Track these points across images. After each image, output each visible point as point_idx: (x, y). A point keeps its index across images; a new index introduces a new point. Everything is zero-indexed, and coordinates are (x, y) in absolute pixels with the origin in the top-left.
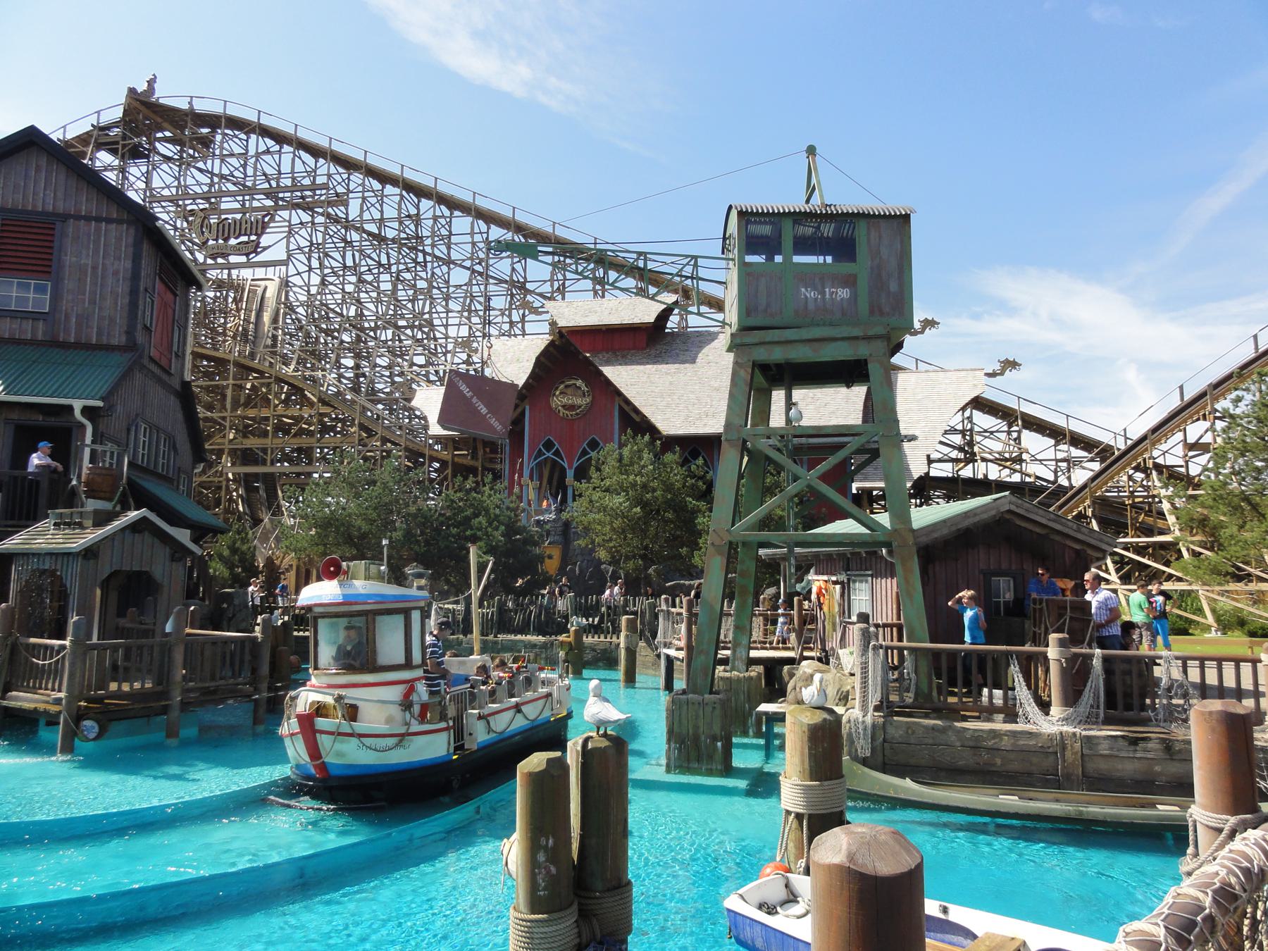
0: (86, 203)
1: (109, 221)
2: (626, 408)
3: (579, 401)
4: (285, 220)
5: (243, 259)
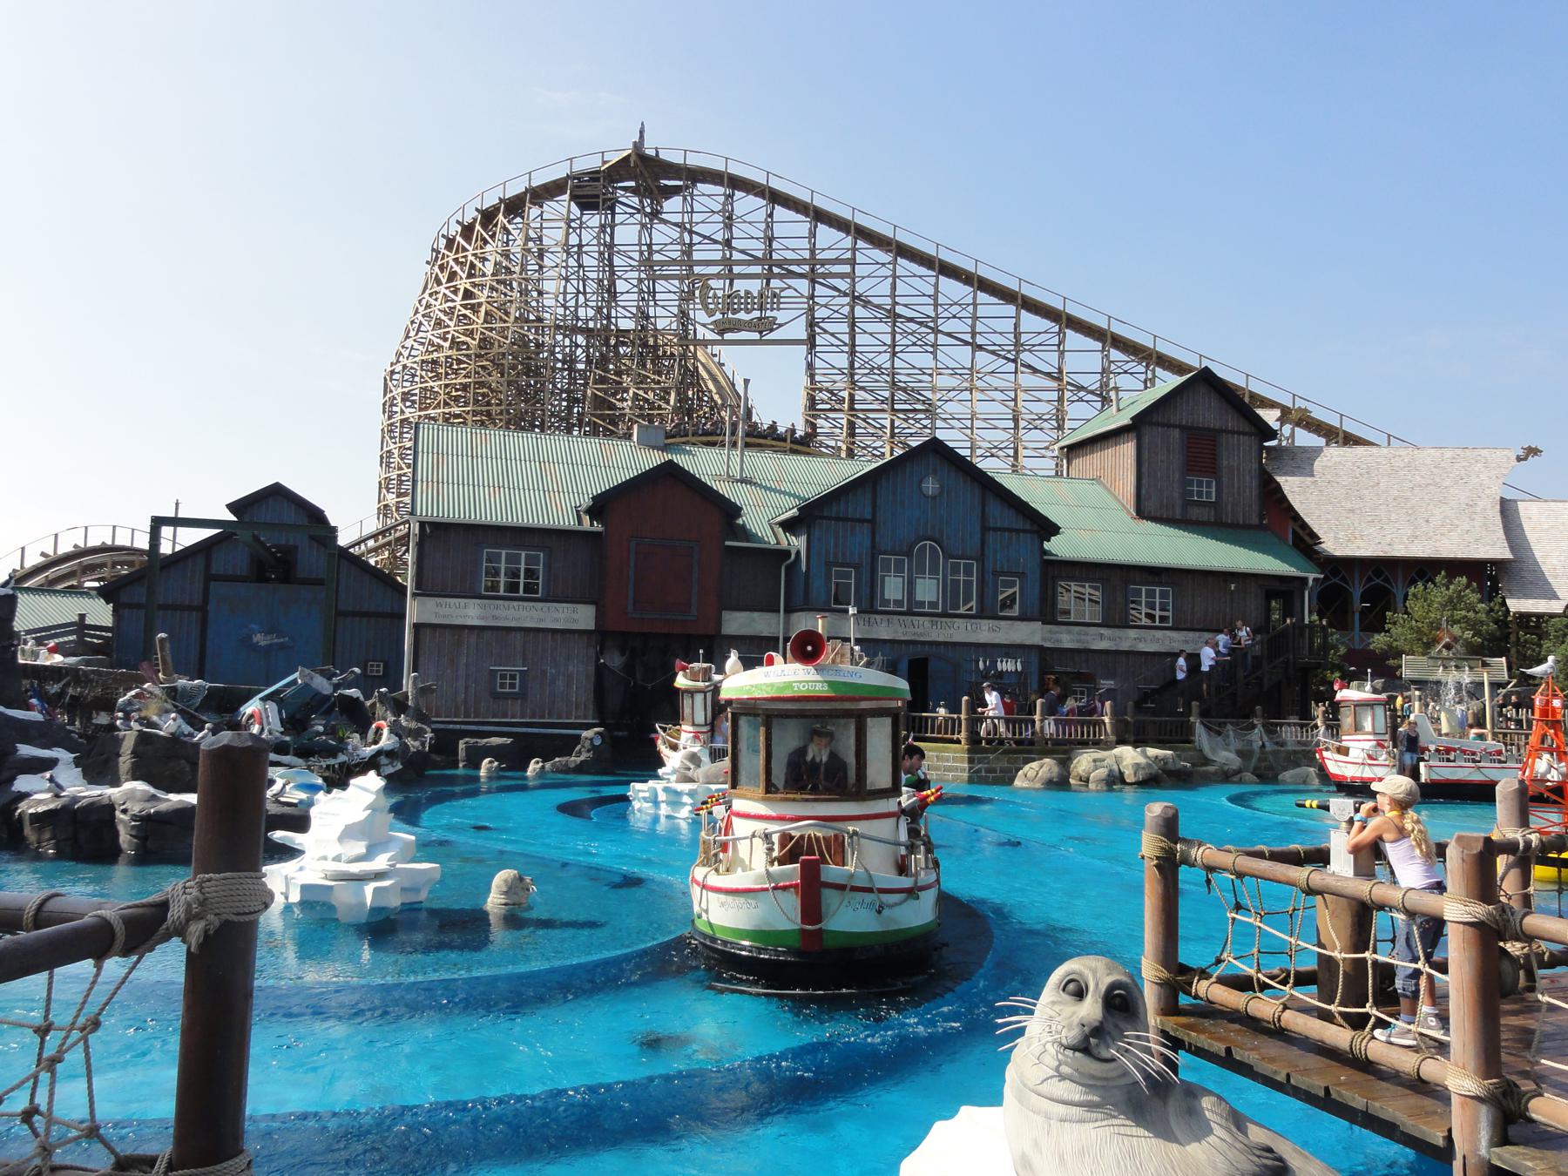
0: (1232, 421)
1: (1244, 434)
2: (1300, 532)
4: (802, 296)
5: (756, 336)
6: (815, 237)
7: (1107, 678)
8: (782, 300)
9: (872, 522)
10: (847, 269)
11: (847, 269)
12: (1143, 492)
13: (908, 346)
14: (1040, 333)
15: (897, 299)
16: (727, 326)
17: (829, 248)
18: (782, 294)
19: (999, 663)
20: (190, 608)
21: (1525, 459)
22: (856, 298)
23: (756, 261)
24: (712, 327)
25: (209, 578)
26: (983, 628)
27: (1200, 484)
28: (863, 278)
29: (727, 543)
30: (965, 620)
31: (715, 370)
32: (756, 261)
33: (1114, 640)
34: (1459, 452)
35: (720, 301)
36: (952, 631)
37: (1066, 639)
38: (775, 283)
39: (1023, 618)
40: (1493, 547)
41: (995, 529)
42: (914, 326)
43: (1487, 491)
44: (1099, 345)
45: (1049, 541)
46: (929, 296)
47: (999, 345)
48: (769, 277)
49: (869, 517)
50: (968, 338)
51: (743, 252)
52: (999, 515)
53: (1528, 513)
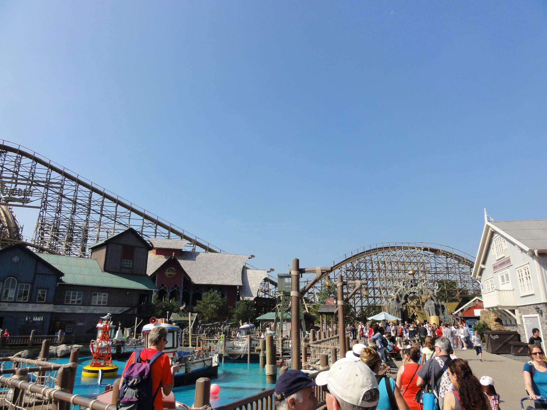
1: (143, 248)
2: (185, 276)
3: (173, 273)
4: (41, 193)
5: (21, 204)
6: (50, 174)
7: (81, 322)
8: (33, 193)
10: (59, 186)
11: (59, 186)
12: (107, 264)
13: (79, 212)
14: (122, 213)
15: (77, 197)
16: (10, 199)
17: (53, 179)
18: (34, 191)
19: (34, 318)
21: (251, 258)
22: (62, 196)
23: (27, 180)
26: (30, 306)
27: (127, 262)
28: (65, 189)
30: (23, 304)
31: (8, 214)
33: (85, 310)
34: (235, 255)
35: (9, 191)
37: (67, 310)
38: (33, 187)
39: (47, 303)
40: (238, 282)
41: (40, 274)
42: (80, 206)
43: (240, 267)
44: (142, 218)
47: (110, 215)
48: (31, 185)
50: (99, 212)
51: (22, 176)
52: (41, 268)
53: (249, 272)
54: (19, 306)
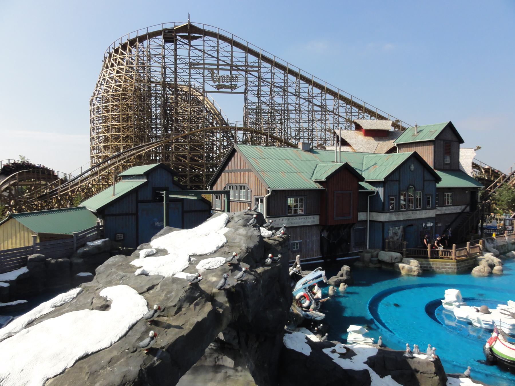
5: (230, 90)
8: (239, 79)
9: (399, 181)
10: (257, 69)
20: (132, 214)
24: (215, 87)
25: (138, 202)
29: (360, 191)
32: (228, 65)
36: (416, 215)
38: (233, 72)
45: (438, 183)
46: (282, 79)
49: (398, 179)
54: (417, 213)
